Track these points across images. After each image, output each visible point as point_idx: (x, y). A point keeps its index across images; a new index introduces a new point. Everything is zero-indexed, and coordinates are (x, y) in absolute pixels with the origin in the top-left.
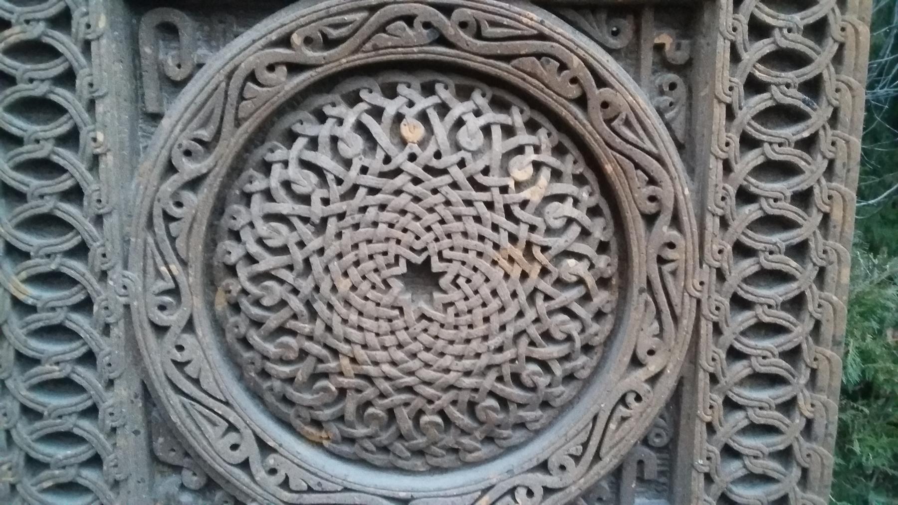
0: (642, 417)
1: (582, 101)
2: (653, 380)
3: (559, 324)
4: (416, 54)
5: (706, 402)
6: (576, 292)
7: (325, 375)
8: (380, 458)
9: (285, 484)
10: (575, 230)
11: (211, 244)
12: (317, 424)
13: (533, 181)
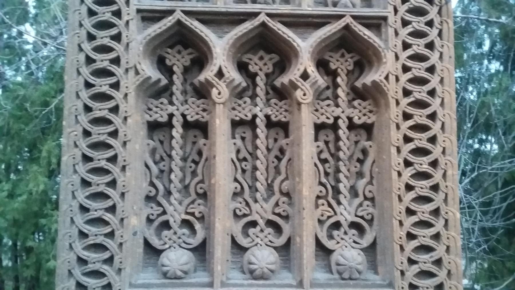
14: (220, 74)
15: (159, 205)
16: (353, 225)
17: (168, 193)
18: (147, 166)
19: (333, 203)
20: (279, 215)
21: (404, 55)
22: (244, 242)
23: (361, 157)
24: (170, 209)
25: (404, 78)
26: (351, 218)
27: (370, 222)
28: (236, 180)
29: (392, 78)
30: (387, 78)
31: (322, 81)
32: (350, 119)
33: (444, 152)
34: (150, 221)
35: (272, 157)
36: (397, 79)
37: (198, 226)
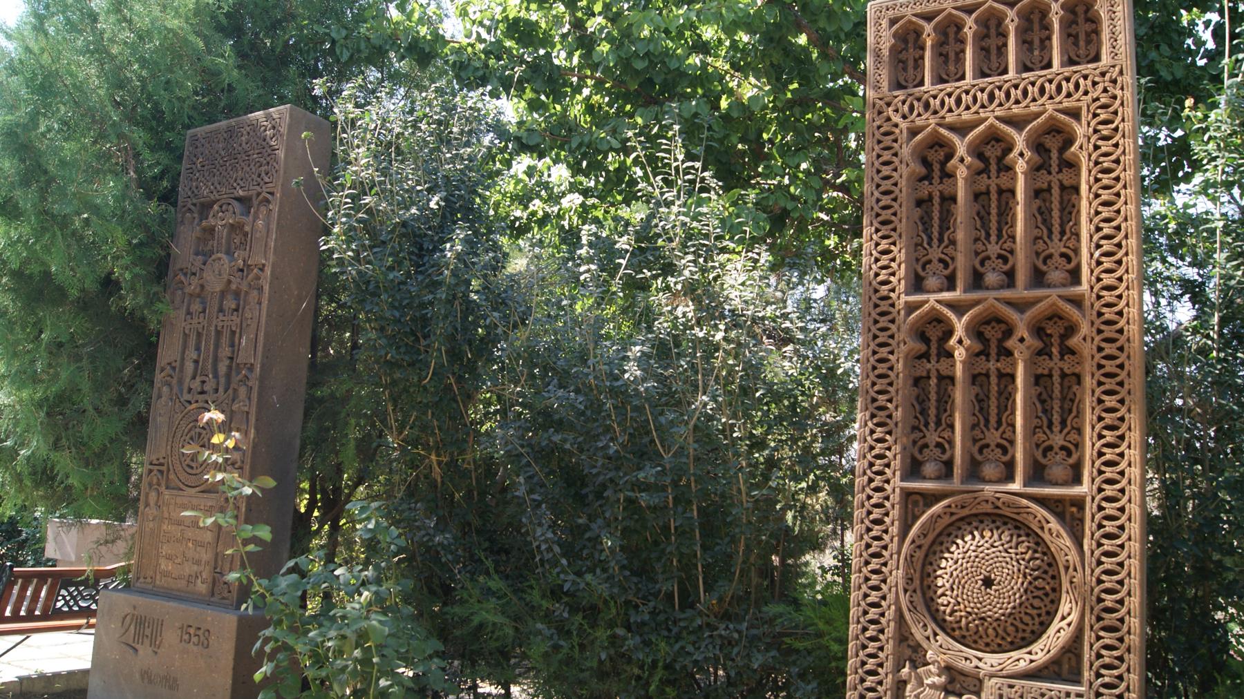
0: (1065, 635)
1: (1042, 528)
2: (1069, 625)
3: (1036, 603)
4: (989, 511)
5: (1088, 636)
11: (923, 566)
12: (953, 630)
14: (960, 342)
15: (921, 431)
16: (1063, 448)
17: (927, 424)
21: (1097, 322)
22: (979, 458)
24: (928, 434)
25: (1097, 339)
26: (1061, 443)
27: (1076, 446)
29: (1089, 340)
30: (1084, 339)
31: (1038, 344)
33: (1129, 393)
34: (915, 442)
35: (1002, 399)
37: (947, 446)
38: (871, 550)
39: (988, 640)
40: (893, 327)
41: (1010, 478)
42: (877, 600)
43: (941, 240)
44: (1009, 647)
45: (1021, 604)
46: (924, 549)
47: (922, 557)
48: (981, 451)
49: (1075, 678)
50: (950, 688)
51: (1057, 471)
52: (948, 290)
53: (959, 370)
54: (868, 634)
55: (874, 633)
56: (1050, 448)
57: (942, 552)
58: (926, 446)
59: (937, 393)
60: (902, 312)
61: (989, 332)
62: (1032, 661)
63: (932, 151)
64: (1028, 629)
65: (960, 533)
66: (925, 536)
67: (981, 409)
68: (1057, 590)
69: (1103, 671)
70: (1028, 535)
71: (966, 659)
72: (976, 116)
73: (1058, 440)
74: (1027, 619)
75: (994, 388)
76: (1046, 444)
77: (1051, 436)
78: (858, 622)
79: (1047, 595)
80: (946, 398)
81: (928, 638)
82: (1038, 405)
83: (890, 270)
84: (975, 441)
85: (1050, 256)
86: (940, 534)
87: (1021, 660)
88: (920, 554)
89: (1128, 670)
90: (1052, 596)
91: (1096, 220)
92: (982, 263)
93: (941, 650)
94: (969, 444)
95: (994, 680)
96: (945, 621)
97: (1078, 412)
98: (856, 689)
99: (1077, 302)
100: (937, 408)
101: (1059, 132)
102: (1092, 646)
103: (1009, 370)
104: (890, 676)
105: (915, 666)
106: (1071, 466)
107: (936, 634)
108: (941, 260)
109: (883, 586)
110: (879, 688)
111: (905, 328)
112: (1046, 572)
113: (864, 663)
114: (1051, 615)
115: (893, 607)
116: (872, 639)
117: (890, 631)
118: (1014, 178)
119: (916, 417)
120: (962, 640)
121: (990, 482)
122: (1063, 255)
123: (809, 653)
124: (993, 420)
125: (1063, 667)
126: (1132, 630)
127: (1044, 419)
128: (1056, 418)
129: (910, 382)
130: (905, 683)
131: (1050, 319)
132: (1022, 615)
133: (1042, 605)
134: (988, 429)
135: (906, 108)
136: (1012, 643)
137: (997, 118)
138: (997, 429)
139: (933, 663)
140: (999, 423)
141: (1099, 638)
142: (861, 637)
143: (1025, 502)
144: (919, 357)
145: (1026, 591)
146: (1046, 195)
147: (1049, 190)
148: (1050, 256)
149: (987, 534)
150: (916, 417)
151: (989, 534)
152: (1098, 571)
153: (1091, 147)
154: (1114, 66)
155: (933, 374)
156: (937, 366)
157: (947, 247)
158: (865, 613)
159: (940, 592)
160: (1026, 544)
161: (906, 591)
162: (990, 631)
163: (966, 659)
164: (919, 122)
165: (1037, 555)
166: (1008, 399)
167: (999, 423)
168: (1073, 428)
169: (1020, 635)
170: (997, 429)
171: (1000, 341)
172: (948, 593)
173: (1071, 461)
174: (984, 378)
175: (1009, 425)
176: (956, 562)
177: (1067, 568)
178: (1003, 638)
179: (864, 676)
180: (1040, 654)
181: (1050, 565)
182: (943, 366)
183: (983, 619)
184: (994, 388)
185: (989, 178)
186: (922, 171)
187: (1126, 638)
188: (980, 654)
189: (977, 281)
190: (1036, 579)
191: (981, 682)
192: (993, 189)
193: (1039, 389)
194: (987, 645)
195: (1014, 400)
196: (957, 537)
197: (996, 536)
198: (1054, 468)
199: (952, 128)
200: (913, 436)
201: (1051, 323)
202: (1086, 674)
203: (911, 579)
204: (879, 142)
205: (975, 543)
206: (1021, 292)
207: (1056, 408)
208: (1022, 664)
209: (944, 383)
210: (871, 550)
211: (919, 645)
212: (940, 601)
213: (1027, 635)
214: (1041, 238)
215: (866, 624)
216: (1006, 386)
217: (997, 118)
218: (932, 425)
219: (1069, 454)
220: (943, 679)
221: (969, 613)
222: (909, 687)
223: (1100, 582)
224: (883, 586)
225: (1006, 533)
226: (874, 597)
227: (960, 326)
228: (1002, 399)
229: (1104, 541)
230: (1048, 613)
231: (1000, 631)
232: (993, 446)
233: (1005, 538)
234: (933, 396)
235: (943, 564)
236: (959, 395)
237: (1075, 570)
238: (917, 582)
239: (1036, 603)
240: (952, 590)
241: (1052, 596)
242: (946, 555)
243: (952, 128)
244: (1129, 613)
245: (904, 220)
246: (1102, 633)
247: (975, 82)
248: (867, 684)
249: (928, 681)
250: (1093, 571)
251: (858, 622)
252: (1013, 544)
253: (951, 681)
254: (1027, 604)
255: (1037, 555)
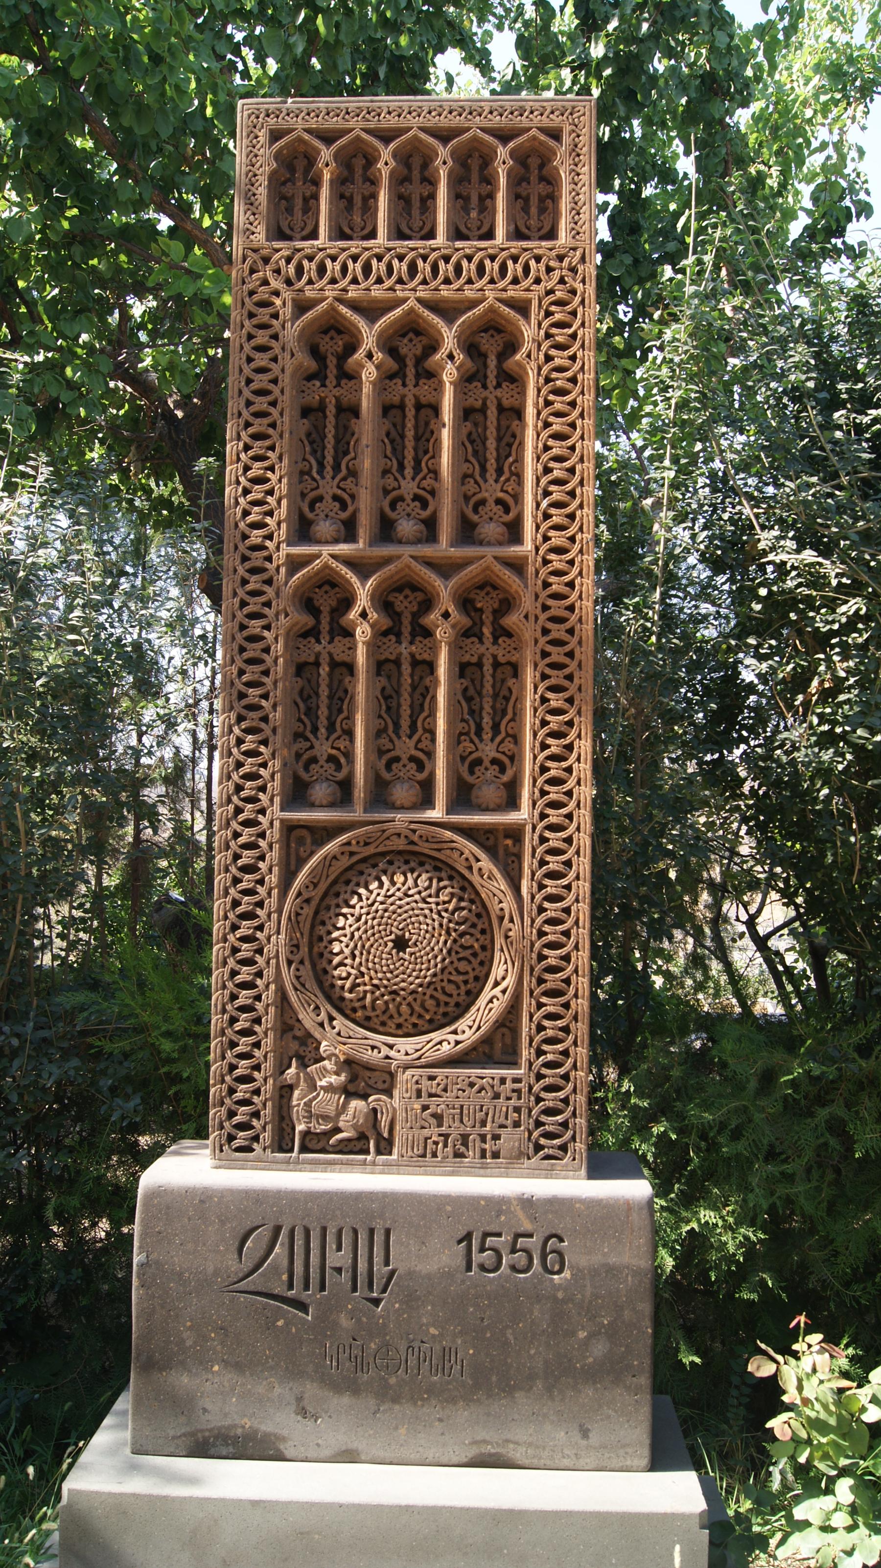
1: (470, 868)
2: (504, 992)
3: (463, 966)
4: (401, 848)
6: (470, 951)
7: (359, 985)
8: (381, 1029)
9: (339, 1034)
10: (468, 924)
11: (313, 927)
12: (354, 1010)
13: (449, 902)
14: (364, 615)
15: (307, 739)
16: (494, 761)
17: (315, 730)
18: (296, 703)
19: (476, 740)
20: (422, 750)
22: (387, 776)
23: (507, 694)
24: (317, 744)
25: (543, 617)
26: (494, 754)
27: (512, 758)
28: (380, 717)
29: (532, 618)
30: (526, 617)
31: (466, 621)
32: (495, 657)
33: (580, 689)
34: (298, 756)
35: (417, 695)
36: (537, 618)
37: (343, 760)
38: (240, 910)
39: (401, 1020)
40: (270, 591)
41: (428, 802)
42: (249, 978)
43: (337, 468)
44: (427, 1027)
45: (443, 970)
46: (314, 903)
47: (311, 914)
48: (388, 766)
49: (510, 1058)
50: (351, 1088)
51: (490, 793)
52: (346, 541)
53: (361, 656)
54: (238, 1026)
55: (247, 1025)
56: (478, 762)
57: (338, 906)
58: (314, 760)
59: (330, 686)
60: (283, 570)
61: (401, 603)
62: (457, 1043)
63: (327, 338)
64: (452, 1002)
65: (362, 879)
66: (315, 885)
67: (389, 709)
68: (488, 948)
69: (545, 1047)
70: (451, 878)
71: (373, 1048)
72: (390, 294)
73: (488, 751)
74: (450, 988)
75: (407, 680)
76: (474, 756)
77: (480, 746)
78: (224, 1011)
79: (475, 955)
80: (340, 694)
81: (321, 1025)
82: (464, 704)
83: (266, 508)
84: (381, 753)
85: (483, 502)
86: (335, 882)
87: (445, 1042)
88: (308, 911)
89: (575, 1043)
90: (482, 956)
91: (545, 457)
92: (393, 506)
93: (339, 1038)
94: (374, 757)
95: (409, 1072)
96: (343, 999)
97: (515, 714)
98: (222, 1104)
99: (517, 566)
100: (329, 708)
101: (499, 331)
102: (531, 1016)
103: (426, 656)
104: (271, 1081)
105: (303, 1065)
106: (504, 784)
107: (331, 1019)
108: (336, 498)
109: (258, 958)
110: (255, 1099)
111: (288, 590)
112: (474, 926)
113: (232, 1067)
114: (481, 980)
115: (272, 987)
116: (244, 1033)
117: (269, 1020)
118: (439, 388)
119: (300, 720)
120: (366, 1024)
121: (402, 808)
122: (499, 502)
123: (126, 1055)
124: (405, 723)
125: (496, 1047)
126: (580, 993)
127: (472, 723)
128: (487, 721)
129: (292, 670)
130: (291, 1088)
131: (481, 587)
132: (445, 984)
133: (469, 969)
134: (399, 737)
135: (291, 269)
136: (431, 1021)
137: (419, 300)
138: (410, 737)
139: (329, 1058)
140: (413, 727)
141: (540, 1005)
142: (228, 1032)
143: (448, 834)
144: (305, 635)
145: (449, 952)
146: (479, 417)
147: (483, 410)
148: (483, 502)
149: (399, 878)
150: (300, 720)
151: (402, 879)
152: (539, 921)
153: (542, 357)
154: (574, 249)
155: (324, 660)
156: (330, 647)
157: (344, 479)
158: (234, 997)
159: (336, 960)
160: (449, 890)
161: (290, 963)
162: (404, 1008)
163: (373, 1048)
164: (310, 293)
165: (463, 904)
166: (424, 696)
167: (413, 727)
168: (508, 735)
169: (442, 1010)
170: (410, 737)
171: (416, 616)
172: (348, 961)
173: (505, 778)
174: (392, 666)
175: (426, 730)
176: (358, 919)
177: (501, 919)
178: (420, 1016)
179: (234, 1085)
180: (469, 1033)
181: (479, 916)
182: (338, 648)
183: (395, 992)
184: (407, 680)
185: (404, 385)
186: (311, 365)
187: (573, 1004)
188: (390, 1040)
189: (385, 531)
190: (462, 935)
191: (392, 1076)
192: (410, 402)
193: (465, 682)
194: (399, 1026)
195: (434, 698)
196: (358, 885)
197: (410, 882)
198: (485, 788)
199: (355, 306)
200: (296, 747)
201: (483, 593)
202: (525, 1053)
203: (297, 946)
204: (251, 315)
205: (383, 892)
206: (444, 547)
207: (487, 708)
208: (445, 1047)
209: (338, 671)
210: (240, 910)
211: (309, 1035)
212: (336, 973)
213: (450, 1009)
214: (471, 476)
215: (235, 1013)
216: (421, 678)
217: (419, 300)
218: (323, 730)
219: (503, 770)
220: (343, 1078)
221: (377, 987)
222: (296, 1093)
223: (541, 934)
224: (258, 958)
225: (424, 876)
226: (245, 974)
227: (363, 593)
228: (417, 695)
229: (547, 882)
230: (476, 978)
231: (417, 1008)
232: (404, 760)
233: (423, 882)
234: (324, 691)
235: (341, 922)
236: (361, 689)
237: (511, 920)
238: (304, 949)
239: (463, 966)
240: (354, 957)
241: (482, 956)
242: (345, 910)
243: (355, 306)
244: (576, 971)
245: (286, 435)
246: (544, 1000)
247: (391, 244)
248: (239, 1095)
249: (323, 1083)
250: (533, 921)
251: (224, 1011)
252: (433, 891)
253: (353, 1078)
254: (451, 969)
255: (463, 904)
